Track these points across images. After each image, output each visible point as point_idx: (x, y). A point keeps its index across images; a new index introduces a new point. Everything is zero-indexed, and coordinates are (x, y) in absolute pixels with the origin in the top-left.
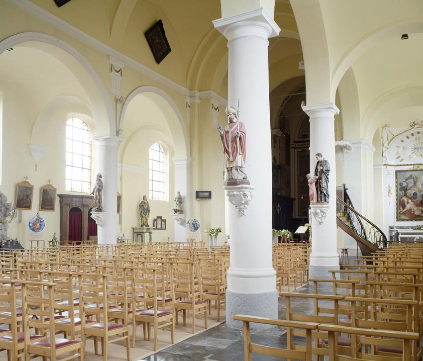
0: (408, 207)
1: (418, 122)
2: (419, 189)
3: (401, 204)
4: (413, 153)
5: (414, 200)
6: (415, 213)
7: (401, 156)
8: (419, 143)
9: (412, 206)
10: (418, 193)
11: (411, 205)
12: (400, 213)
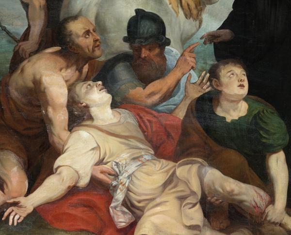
0: (79, 157)
5: (138, 92)
10: (177, 24)
11: (111, 145)
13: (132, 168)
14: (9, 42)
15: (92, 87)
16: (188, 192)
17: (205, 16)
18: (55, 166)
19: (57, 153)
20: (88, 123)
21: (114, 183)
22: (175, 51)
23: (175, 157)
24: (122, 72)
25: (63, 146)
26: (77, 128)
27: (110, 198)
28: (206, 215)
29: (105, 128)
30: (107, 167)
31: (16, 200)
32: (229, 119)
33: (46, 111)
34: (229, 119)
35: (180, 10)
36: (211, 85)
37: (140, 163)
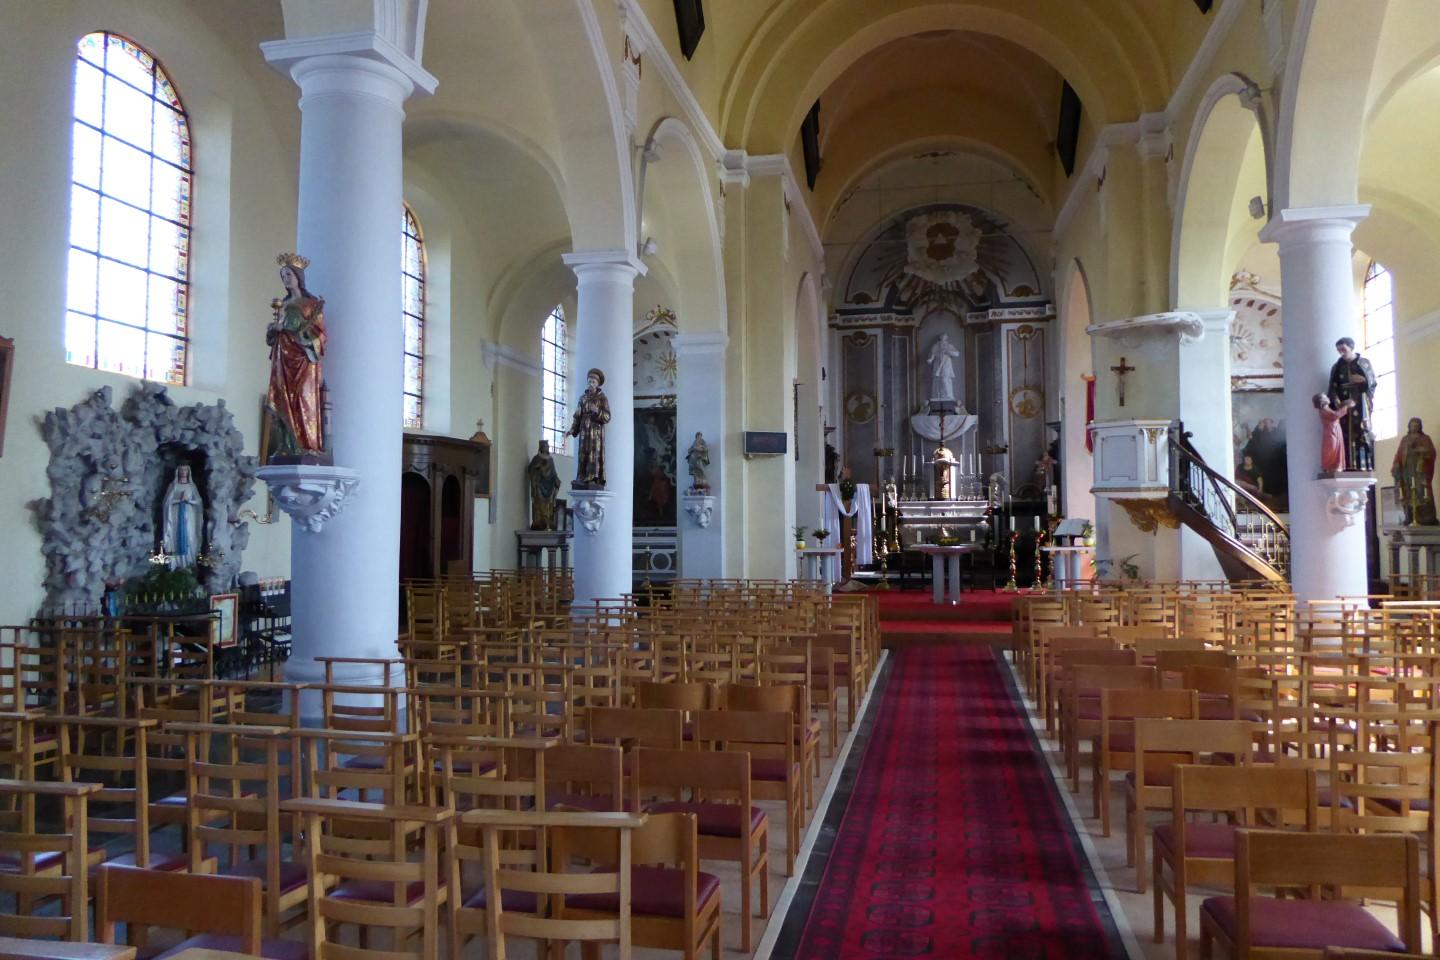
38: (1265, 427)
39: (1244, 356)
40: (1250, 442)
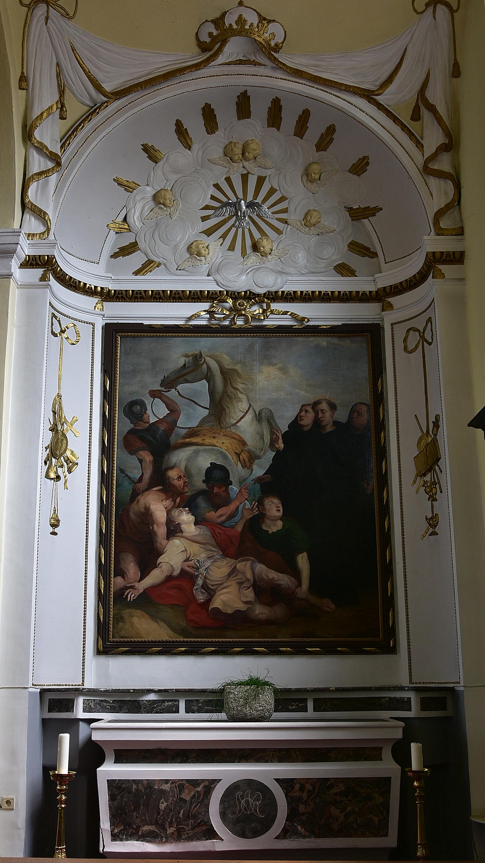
0: (174, 556)
1: (241, 21)
2: (243, 443)
3: (125, 536)
4: (209, 232)
5: (212, 515)
6: (217, 603)
7: (142, 244)
8: (245, 178)
9: (200, 554)
10: (237, 471)
11: (194, 548)
12: (120, 595)
13: (208, 564)
14: (130, 483)
15: (182, 512)
16: (244, 579)
17: (254, 467)
18: (158, 563)
19: (160, 553)
20: (179, 534)
21: (196, 573)
22: (235, 488)
23: (235, 557)
24: (201, 502)
25: (163, 550)
26: (172, 538)
27: (194, 583)
28: (256, 594)
29: (190, 538)
30: (191, 563)
31: (132, 585)
32: (270, 531)
33: (153, 527)
34: (270, 531)
35: (239, 463)
36: (258, 510)
37: (213, 560)
38: (317, 423)
39: (266, 245)
40: (279, 457)
